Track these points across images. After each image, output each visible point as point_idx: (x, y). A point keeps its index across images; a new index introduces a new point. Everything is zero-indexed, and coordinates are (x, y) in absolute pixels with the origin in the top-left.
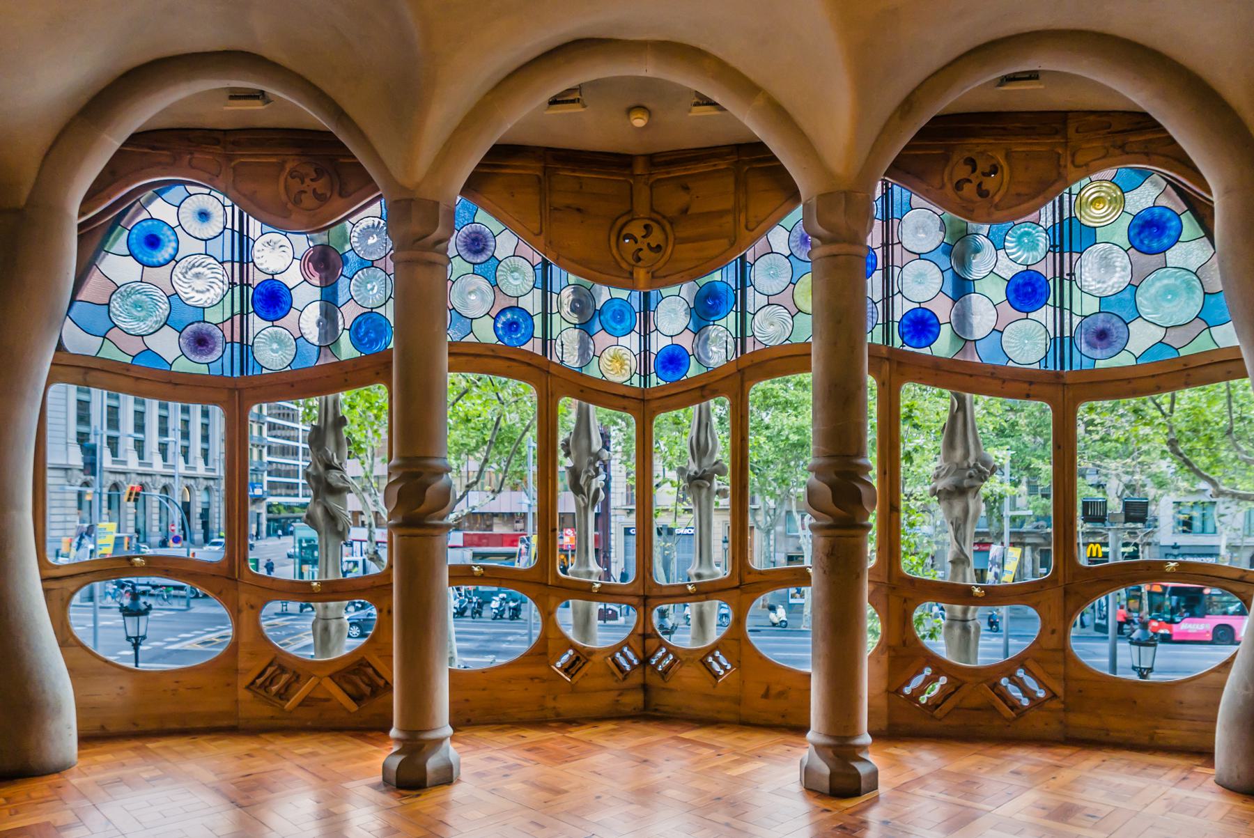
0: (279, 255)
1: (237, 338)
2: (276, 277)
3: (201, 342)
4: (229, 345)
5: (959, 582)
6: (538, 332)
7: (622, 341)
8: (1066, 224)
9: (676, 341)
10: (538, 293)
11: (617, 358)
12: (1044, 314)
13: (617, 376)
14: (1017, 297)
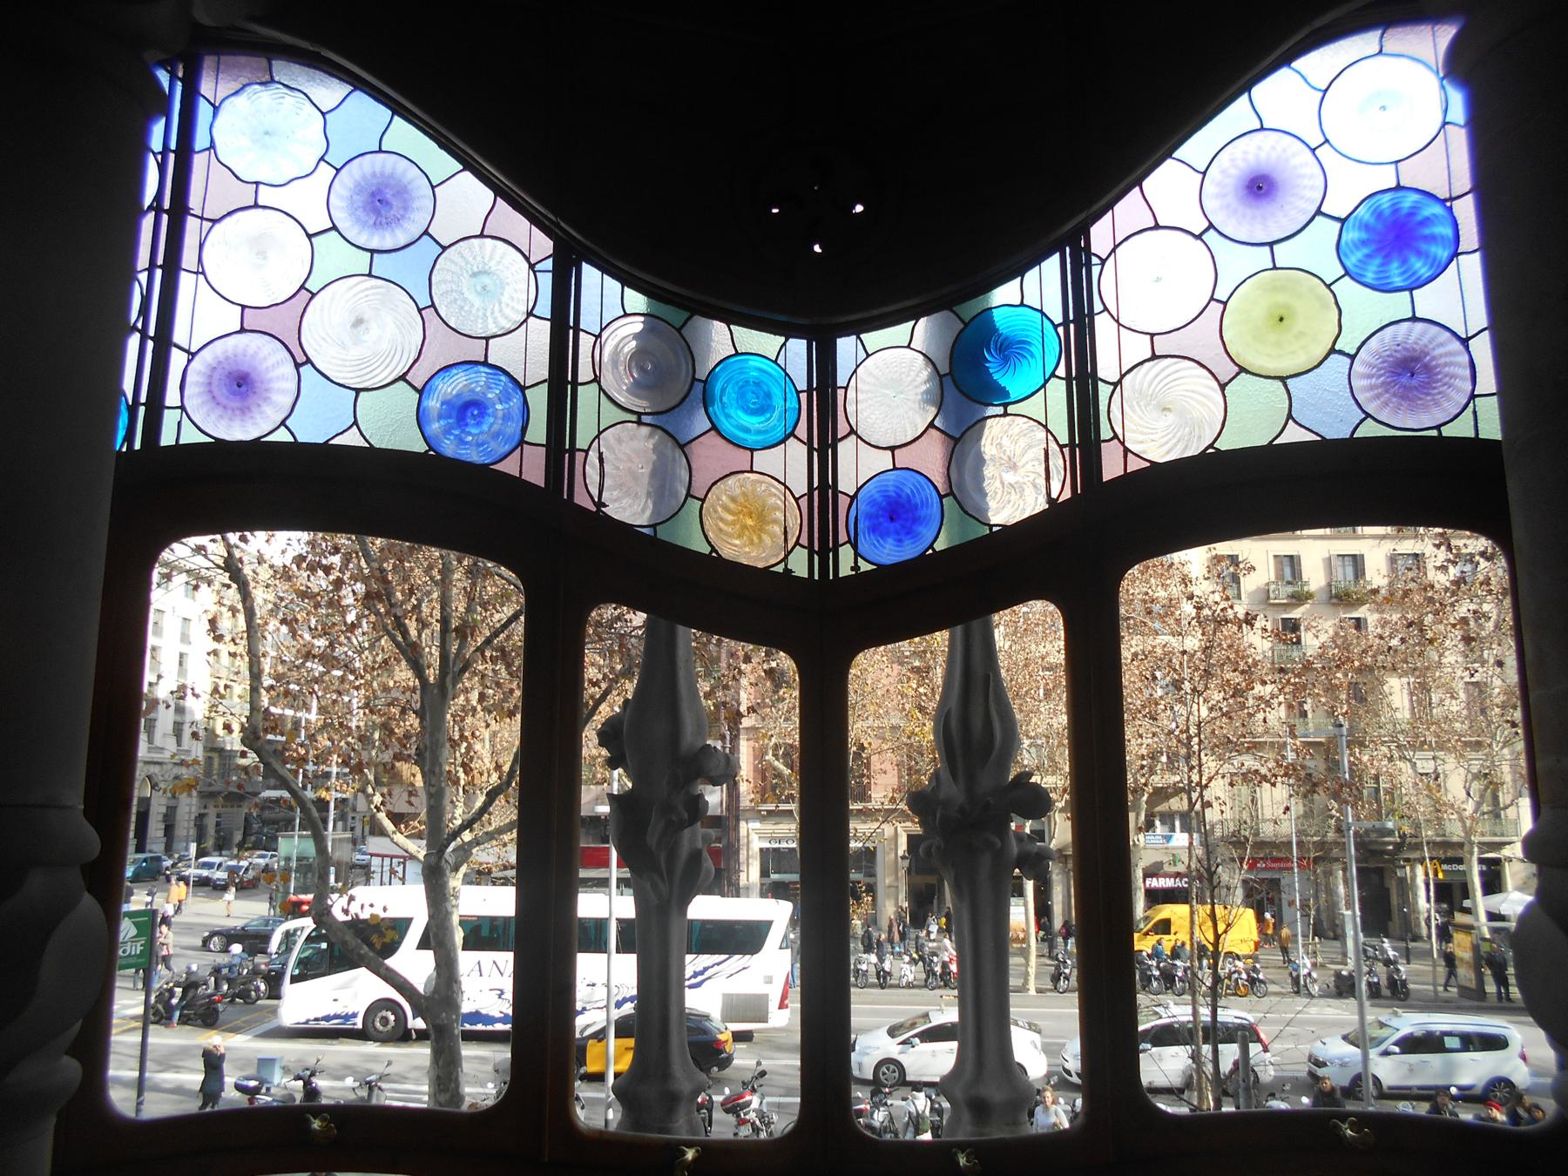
6: (538, 431)
7: (763, 460)
9: (903, 458)
11: (751, 513)
13: (750, 549)
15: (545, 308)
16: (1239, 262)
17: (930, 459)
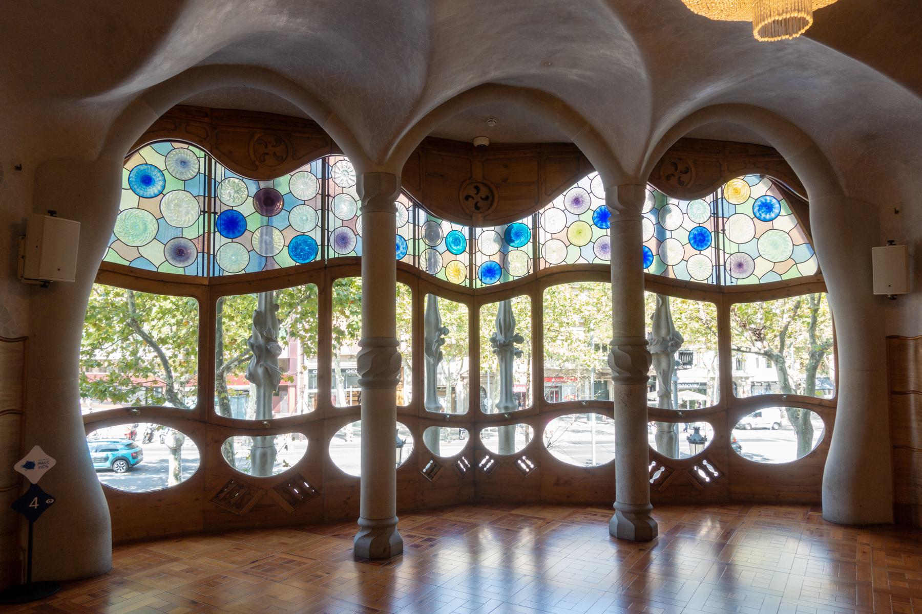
0: (236, 192)
1: (206, 251)
2: (235, 208)
3: (180, 253)
4: (200, 255)
5: (665, 407)
8: (720, 201)
10: (411, 226)
11: (453, 270)
12: (709, 252)
14: (695, 242)
15: (411, 220)
16: (571, 218)
17: (497, 259)
